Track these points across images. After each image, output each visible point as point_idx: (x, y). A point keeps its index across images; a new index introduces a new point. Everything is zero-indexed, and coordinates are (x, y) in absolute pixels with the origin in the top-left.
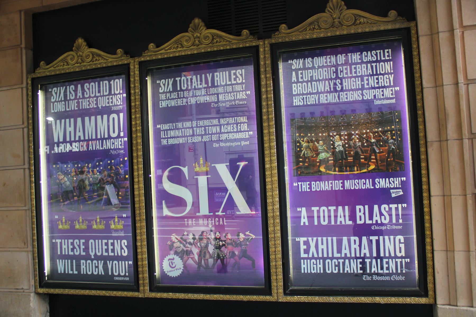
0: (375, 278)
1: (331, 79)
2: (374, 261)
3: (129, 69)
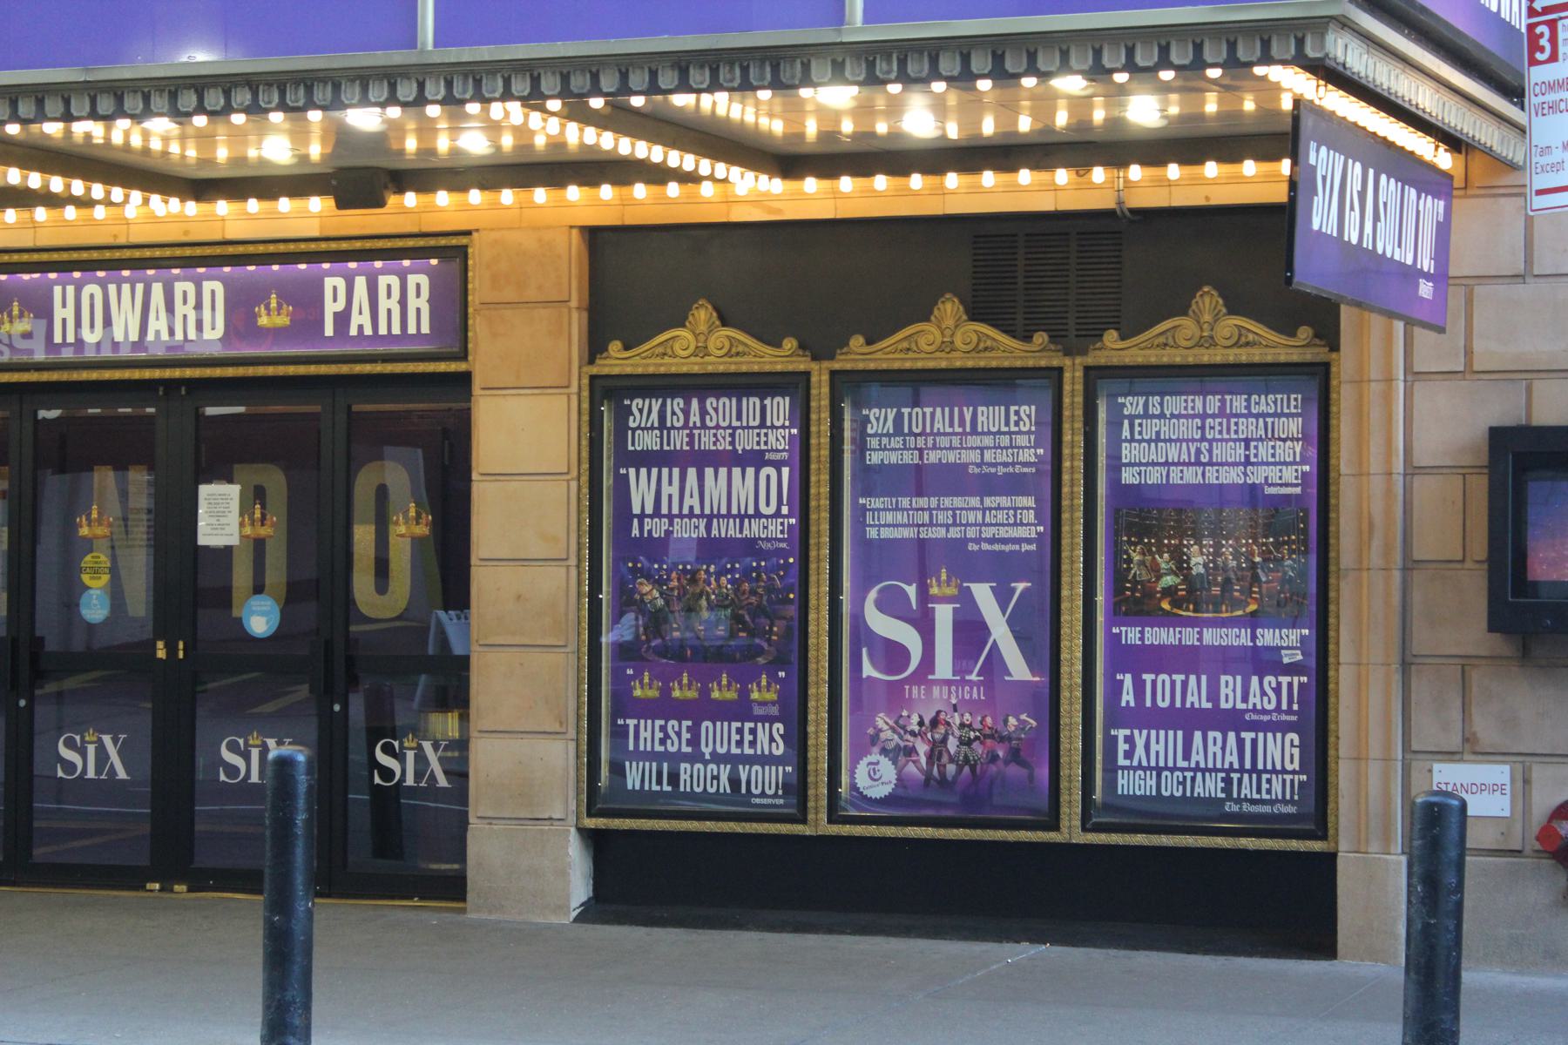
0: (1246, 808)
1: (1193, 440)
2: (1246, 776)
3: (808, 381)
